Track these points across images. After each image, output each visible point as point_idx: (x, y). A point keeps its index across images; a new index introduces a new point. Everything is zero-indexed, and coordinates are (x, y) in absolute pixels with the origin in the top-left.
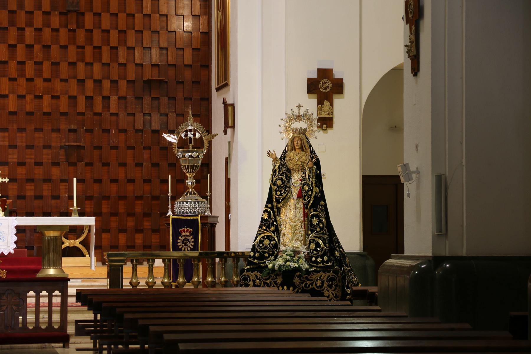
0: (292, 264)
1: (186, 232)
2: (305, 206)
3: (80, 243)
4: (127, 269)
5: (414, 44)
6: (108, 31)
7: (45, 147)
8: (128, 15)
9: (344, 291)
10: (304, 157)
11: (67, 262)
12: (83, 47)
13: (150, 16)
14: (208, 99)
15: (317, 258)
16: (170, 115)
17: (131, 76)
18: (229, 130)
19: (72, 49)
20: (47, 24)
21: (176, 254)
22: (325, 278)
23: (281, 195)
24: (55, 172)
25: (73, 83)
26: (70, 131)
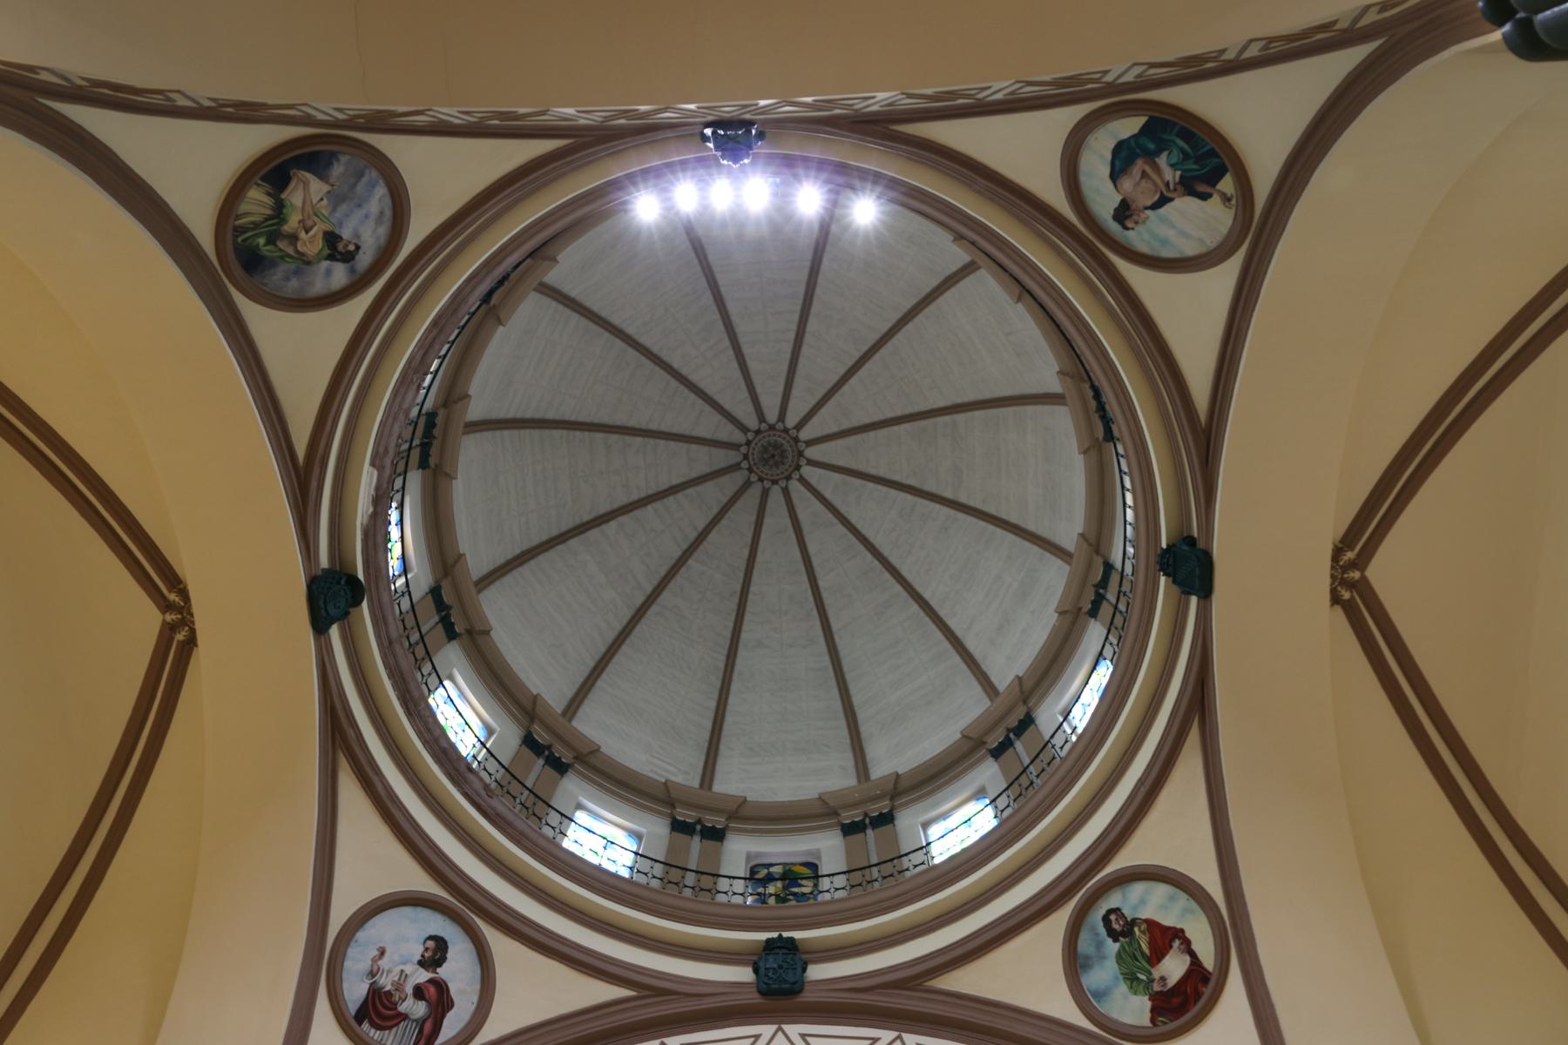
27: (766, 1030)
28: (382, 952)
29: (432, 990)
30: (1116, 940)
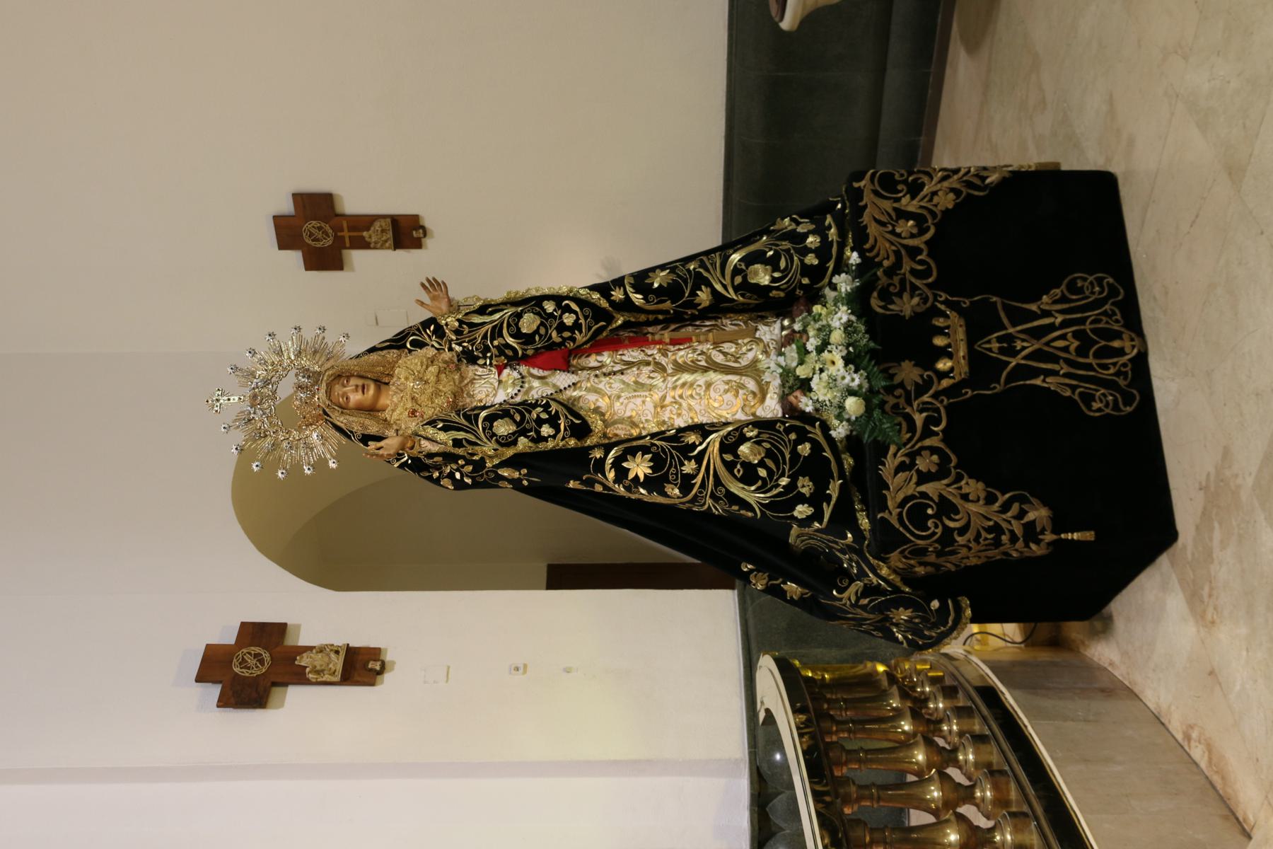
10: (409, 365)
15: (805, 251)
22: (887, 205)
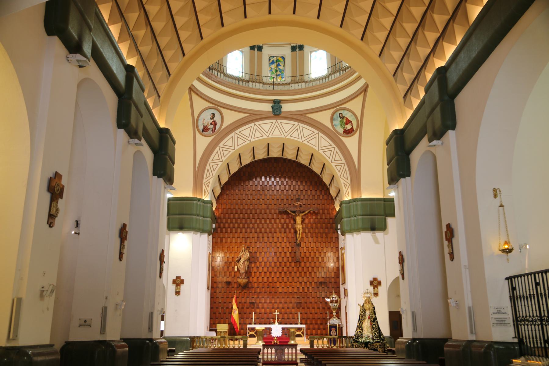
0: (368, 340)
1: (333, 329)
2: (371, 321)
3: (301, 333)
4: (315, 341)
5: (402, 270)
6: (308, 267)
7: (290, 303)
8: (314, 262)
9: (384, 349)
10: (370, 305)
11: (297, 339)
12: (301, 272)
13: (321, 262)
14: (339, 287)
15: (375, 338)
16: (328, 292)
17: (316, 281)
18: (346, 297)
19: (298, 273)
20: (290, 266)
21: (331, 337)
23: (363, 318)
24: (293, 311)
25: (298, 283)
26: (298, 298)
27: (274, 121)
28: (204, 120)
29: (213, 123)
30: (340, 118)
